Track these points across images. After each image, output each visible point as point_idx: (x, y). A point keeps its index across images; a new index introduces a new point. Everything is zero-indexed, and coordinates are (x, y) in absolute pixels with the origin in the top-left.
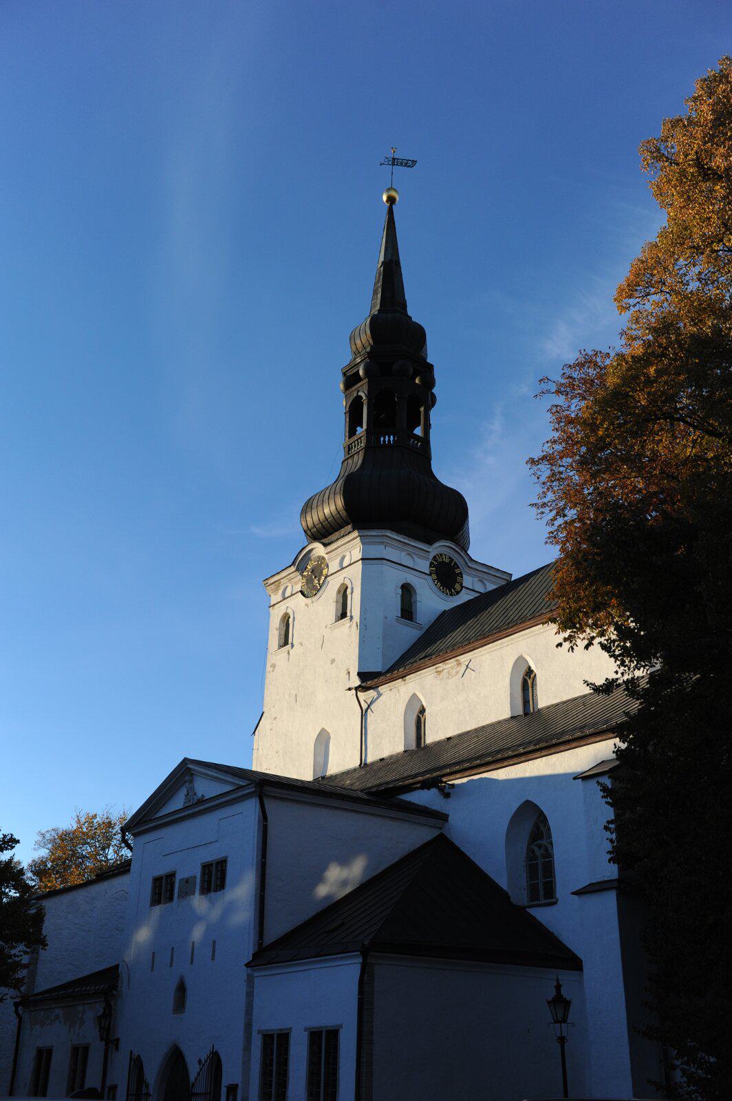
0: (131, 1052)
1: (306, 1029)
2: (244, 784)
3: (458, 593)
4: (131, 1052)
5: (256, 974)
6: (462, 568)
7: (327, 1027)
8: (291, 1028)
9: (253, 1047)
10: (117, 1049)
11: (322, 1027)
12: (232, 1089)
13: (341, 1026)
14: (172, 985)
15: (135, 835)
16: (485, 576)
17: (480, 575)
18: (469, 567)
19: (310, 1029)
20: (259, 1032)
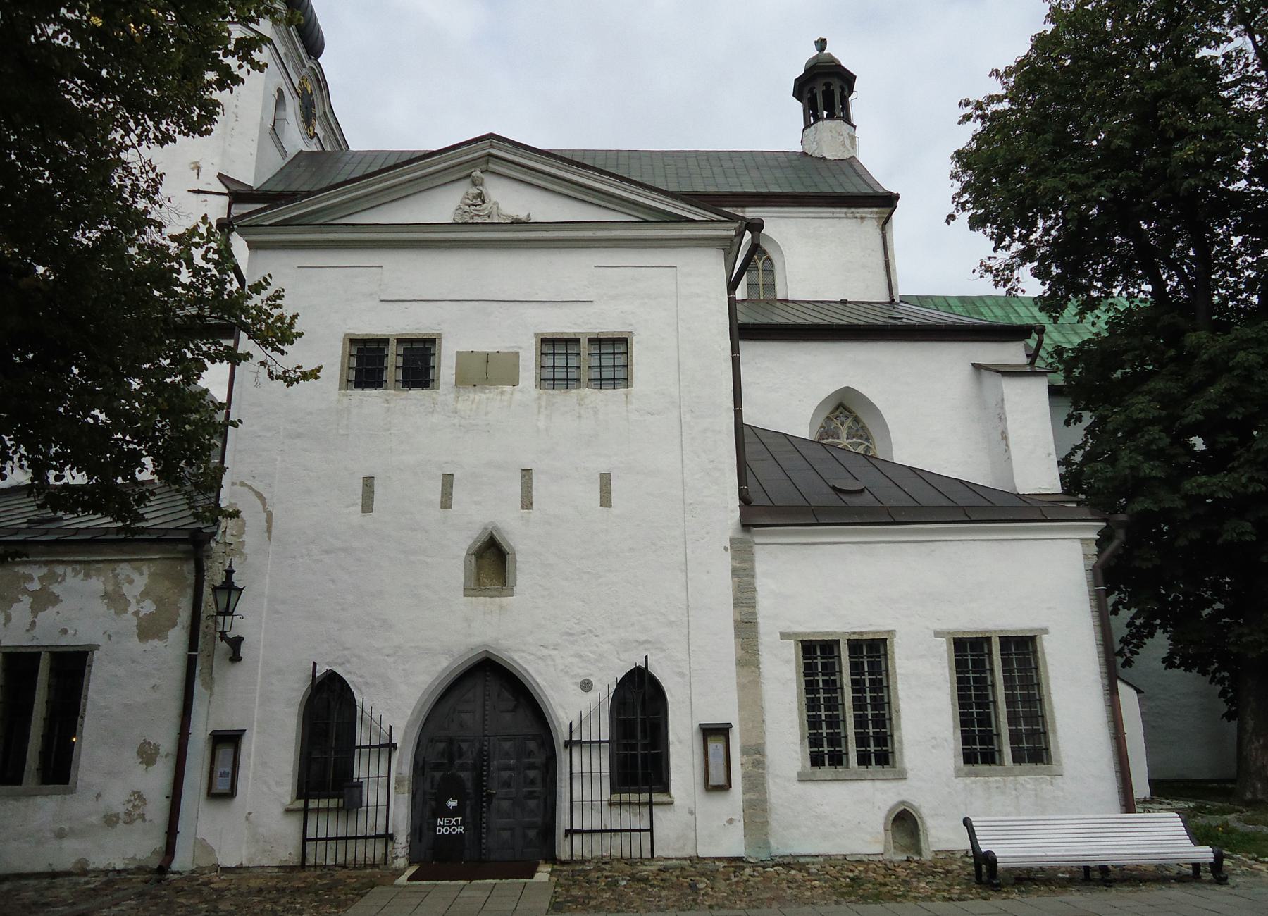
0: (315, 664)
1: (938, 634)
2: (697, 218)
3: (312, 138)
4: (315, 664)
5: (757, 540)
6: (318, 111)
7: (1002, 631)
8: (892, 632)
9: (766, 659)
10: (236, 658)
11: (990, 631)
12: (714, 732)
13: (1045, 631)
14: (462, 542)
15: (253, 246)
16: (331, 136)
17: (329, 131)
18: (325, 113)
19: (949, 633)
20: (784, 636)
